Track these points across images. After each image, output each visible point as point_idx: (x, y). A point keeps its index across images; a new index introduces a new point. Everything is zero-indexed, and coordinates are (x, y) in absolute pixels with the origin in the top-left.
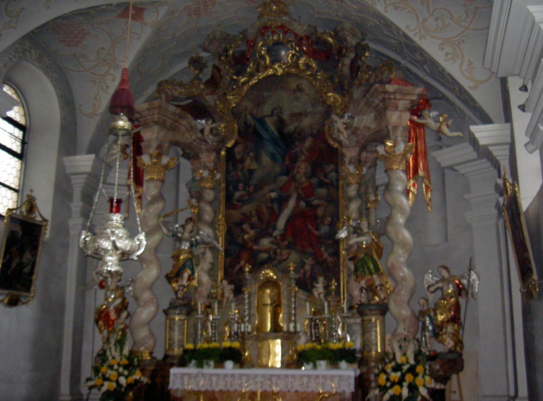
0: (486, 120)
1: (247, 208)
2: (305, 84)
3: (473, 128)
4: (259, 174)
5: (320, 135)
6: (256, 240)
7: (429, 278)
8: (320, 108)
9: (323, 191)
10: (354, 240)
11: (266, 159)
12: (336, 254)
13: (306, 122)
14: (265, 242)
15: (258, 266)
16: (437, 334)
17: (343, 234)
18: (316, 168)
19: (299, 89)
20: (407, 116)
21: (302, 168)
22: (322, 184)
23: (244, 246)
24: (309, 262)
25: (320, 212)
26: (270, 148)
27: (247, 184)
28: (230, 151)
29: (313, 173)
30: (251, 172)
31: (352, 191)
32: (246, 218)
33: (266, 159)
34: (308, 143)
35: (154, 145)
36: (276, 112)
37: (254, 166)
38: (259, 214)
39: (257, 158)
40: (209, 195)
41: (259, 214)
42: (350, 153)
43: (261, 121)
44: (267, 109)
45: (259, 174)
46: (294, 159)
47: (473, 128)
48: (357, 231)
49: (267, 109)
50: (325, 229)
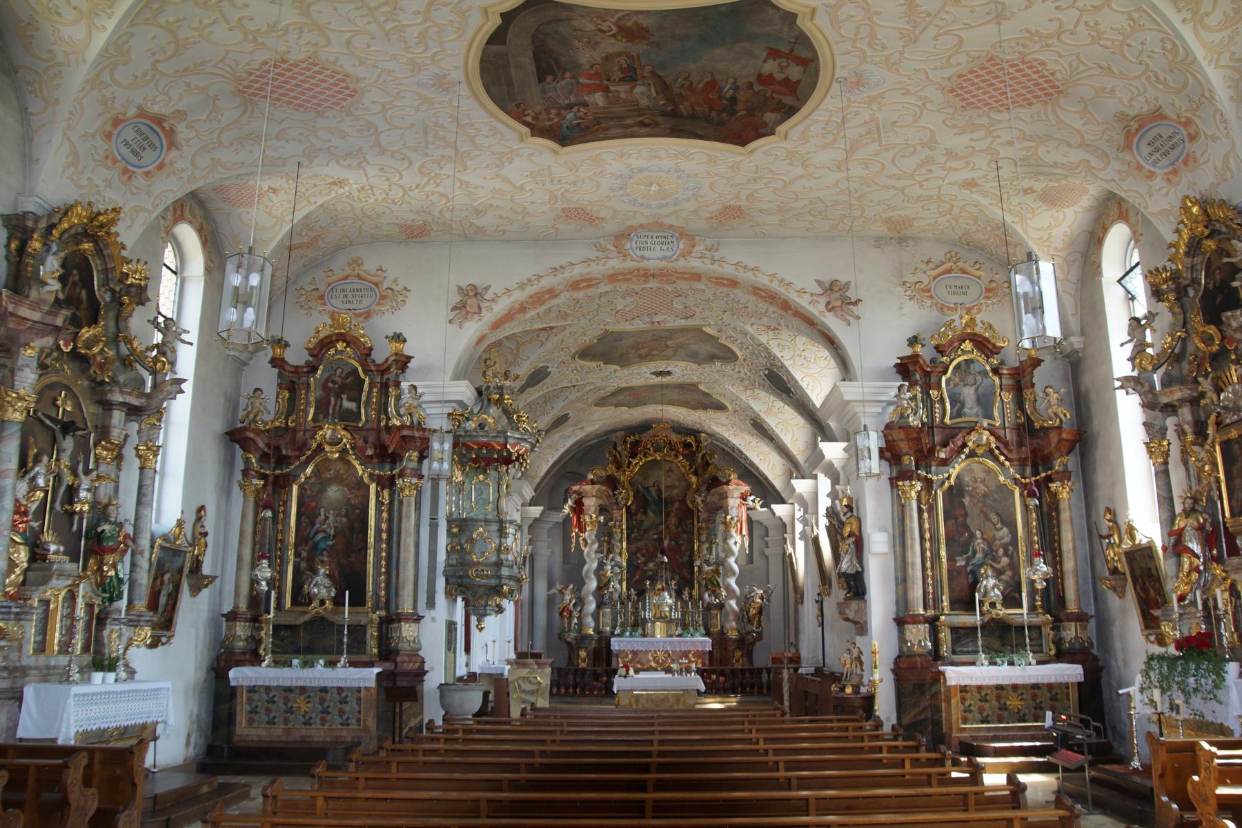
0: (783, 502)
1: (639, 544)
2: (674, 468)
3: (773, 506)
4: (647, 523)
5: (683, 502)
6: (645, 563)
7: (746, 590)
8: (683, 484)
9: (685, 536)
10: (706, 568)
11: (651, 514)
12: (692, 573)
13: (675, 492)
14: (651, 565)
15: (653, 580)
16: (750, 621)
17: (698, 563)
18: (681, 521)
19: (670, 470)
20: (739, 501)
21: (673, 520)
22: (684, 531)
23: (638, 567)
24: (677, 577)
25: (683, 548)
26: (653, 507)
27: (639, 529)
28: (628, 509)
29: (679, 525)
30: (642, 521)
31: (703, 538)
32: (639, 550)
33: (651, 514)
34: (676, 505)
35: (593, 509)
36: (657, 484)
37: (643, 518)
38: (647, 547)
39: (645, 513)
40: (618, 537)
41: (647, 547)
42: (703, 516)
43: (647, 489)
44: (651, 483)
45: (647, 523)
46: (668, 515)
47: (773, 506)
48: (707, 562)
49: (651, 483)
50: (686, 559)
